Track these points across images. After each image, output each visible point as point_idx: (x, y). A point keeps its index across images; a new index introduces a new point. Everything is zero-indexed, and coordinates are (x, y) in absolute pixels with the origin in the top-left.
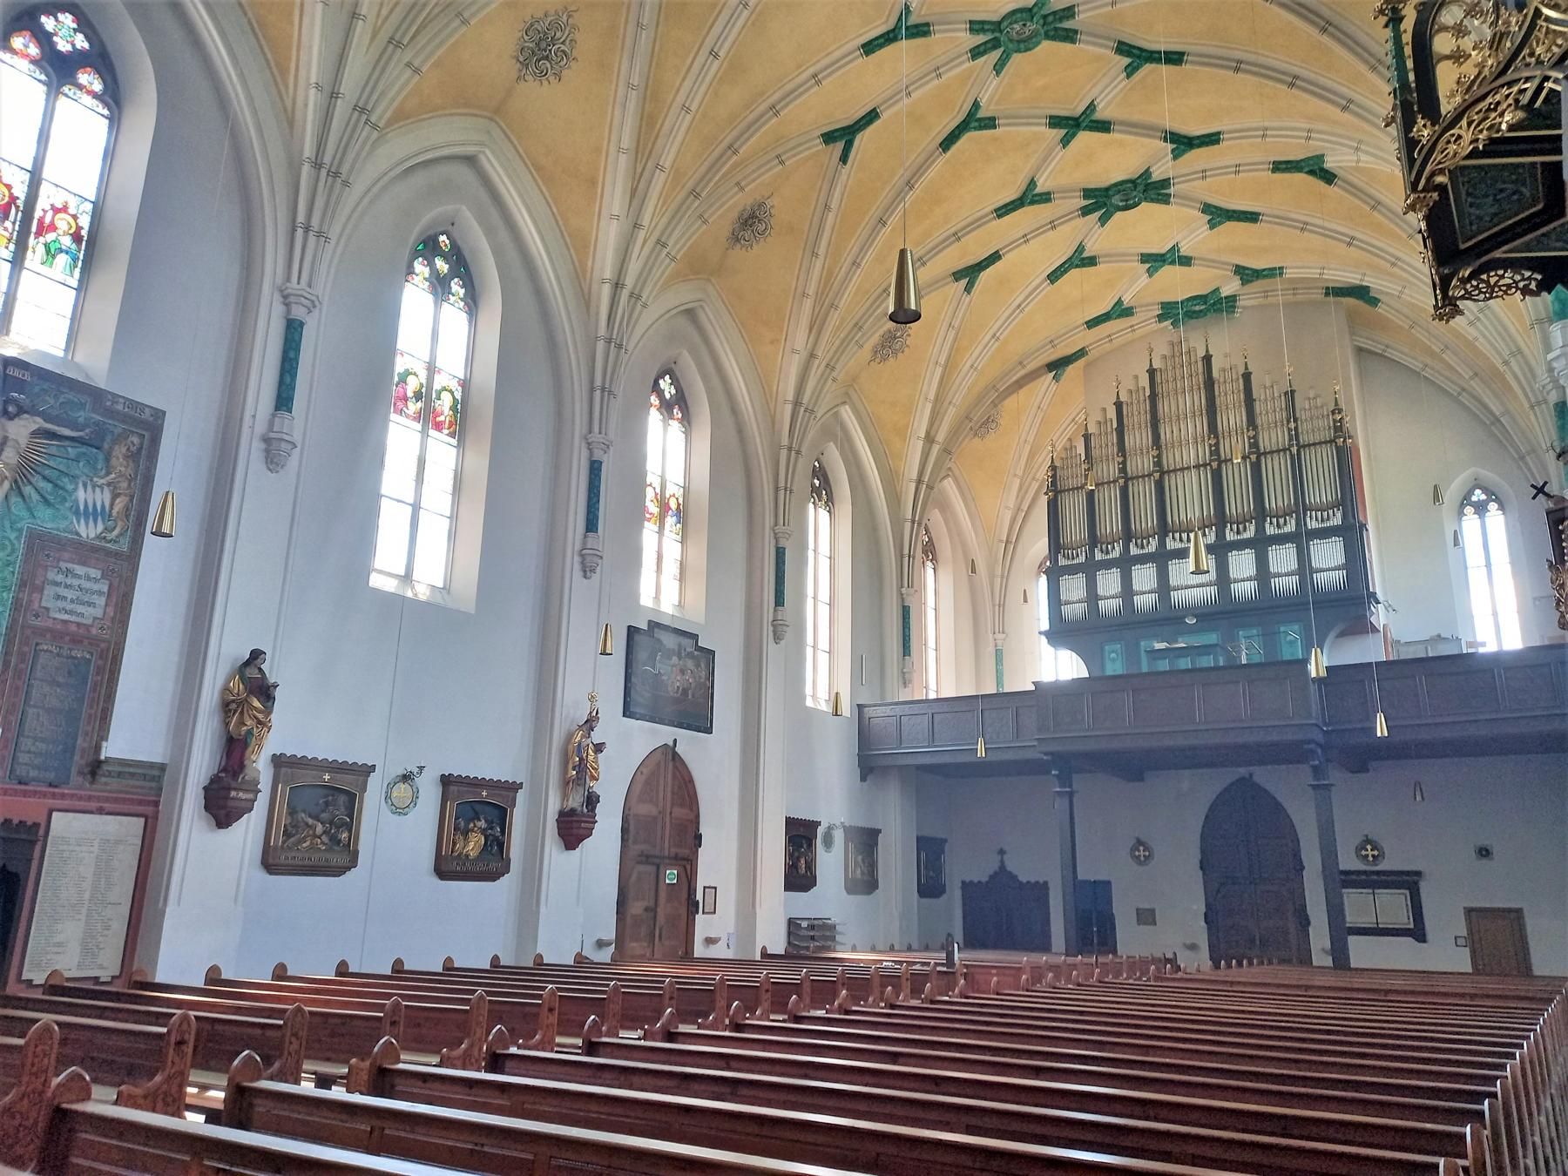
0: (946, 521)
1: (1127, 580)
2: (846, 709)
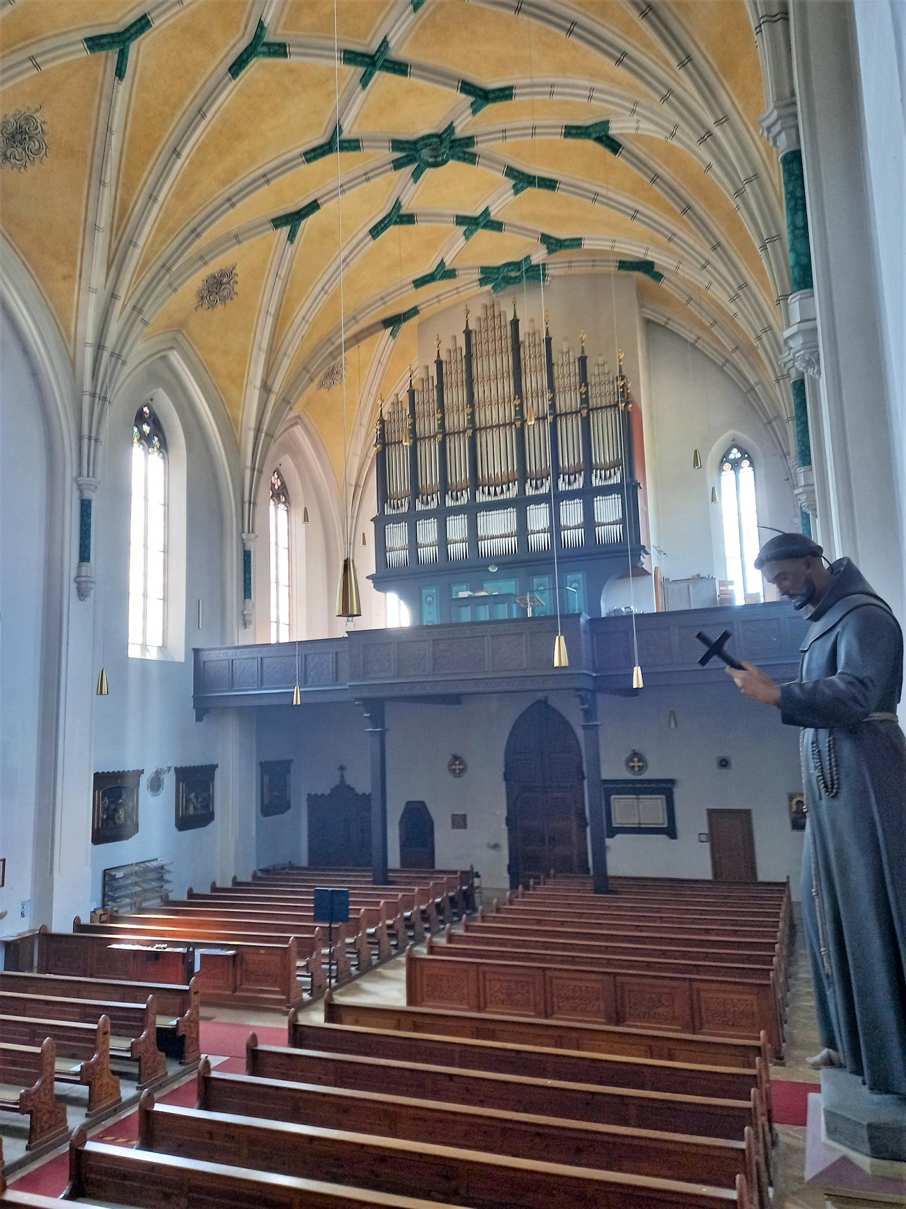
0: (298, 466)
2: (179, 654)
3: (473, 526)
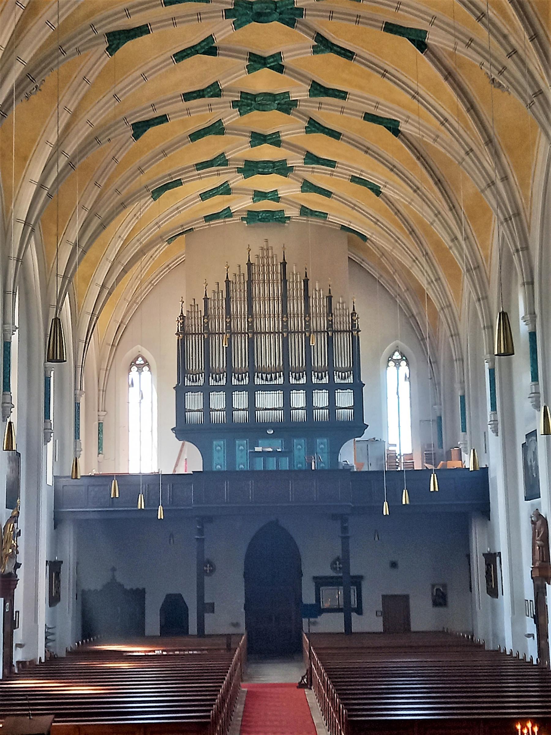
1: (229, 401)
3: (252, 400)
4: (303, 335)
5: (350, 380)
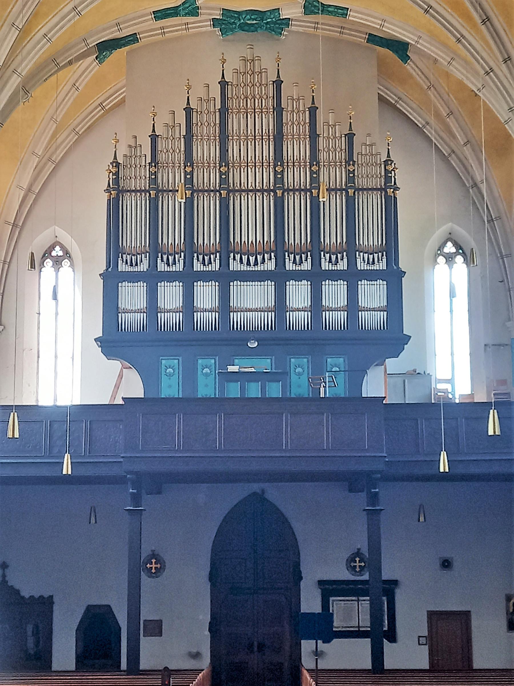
4: (308, 193)
5: (382, 265)
